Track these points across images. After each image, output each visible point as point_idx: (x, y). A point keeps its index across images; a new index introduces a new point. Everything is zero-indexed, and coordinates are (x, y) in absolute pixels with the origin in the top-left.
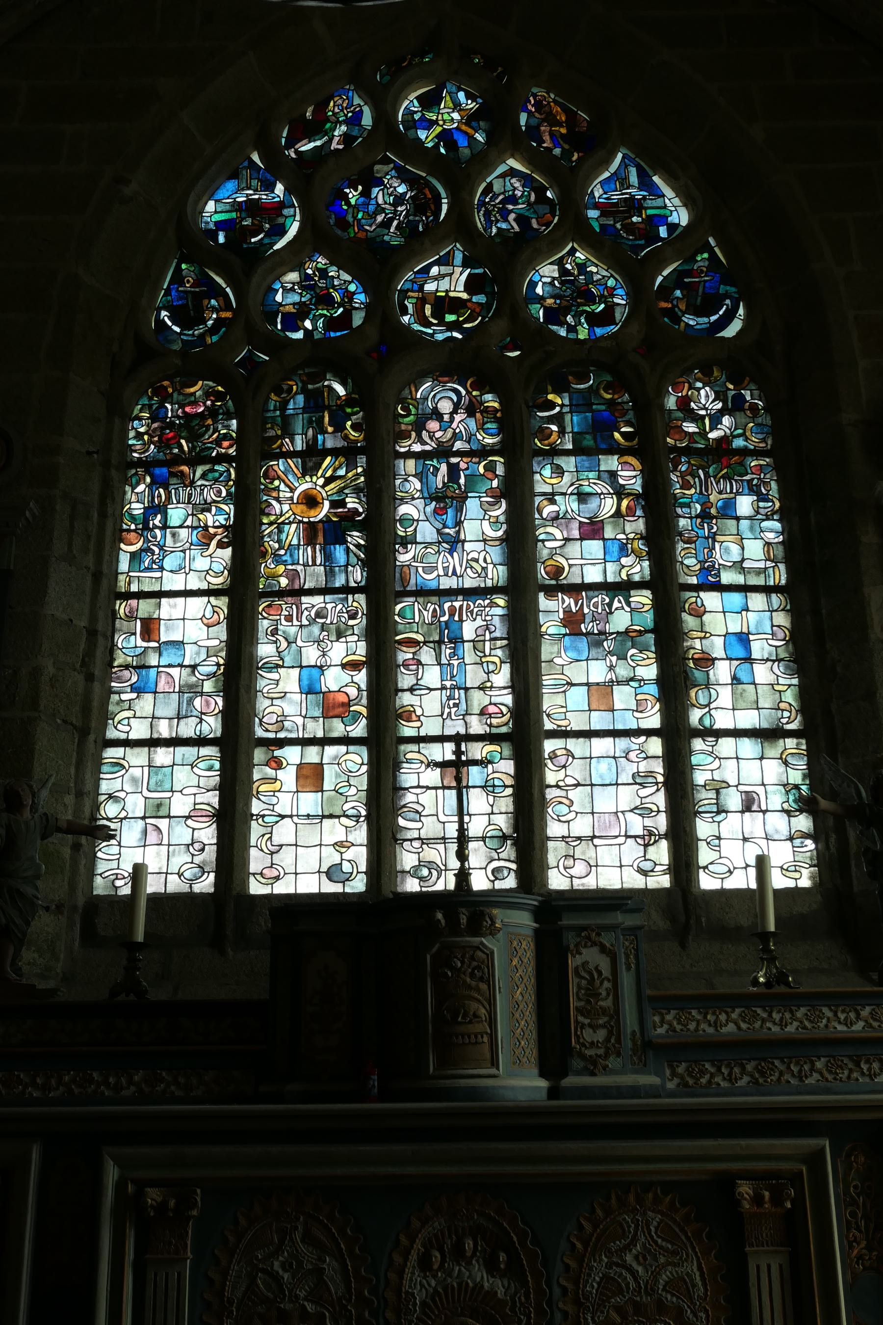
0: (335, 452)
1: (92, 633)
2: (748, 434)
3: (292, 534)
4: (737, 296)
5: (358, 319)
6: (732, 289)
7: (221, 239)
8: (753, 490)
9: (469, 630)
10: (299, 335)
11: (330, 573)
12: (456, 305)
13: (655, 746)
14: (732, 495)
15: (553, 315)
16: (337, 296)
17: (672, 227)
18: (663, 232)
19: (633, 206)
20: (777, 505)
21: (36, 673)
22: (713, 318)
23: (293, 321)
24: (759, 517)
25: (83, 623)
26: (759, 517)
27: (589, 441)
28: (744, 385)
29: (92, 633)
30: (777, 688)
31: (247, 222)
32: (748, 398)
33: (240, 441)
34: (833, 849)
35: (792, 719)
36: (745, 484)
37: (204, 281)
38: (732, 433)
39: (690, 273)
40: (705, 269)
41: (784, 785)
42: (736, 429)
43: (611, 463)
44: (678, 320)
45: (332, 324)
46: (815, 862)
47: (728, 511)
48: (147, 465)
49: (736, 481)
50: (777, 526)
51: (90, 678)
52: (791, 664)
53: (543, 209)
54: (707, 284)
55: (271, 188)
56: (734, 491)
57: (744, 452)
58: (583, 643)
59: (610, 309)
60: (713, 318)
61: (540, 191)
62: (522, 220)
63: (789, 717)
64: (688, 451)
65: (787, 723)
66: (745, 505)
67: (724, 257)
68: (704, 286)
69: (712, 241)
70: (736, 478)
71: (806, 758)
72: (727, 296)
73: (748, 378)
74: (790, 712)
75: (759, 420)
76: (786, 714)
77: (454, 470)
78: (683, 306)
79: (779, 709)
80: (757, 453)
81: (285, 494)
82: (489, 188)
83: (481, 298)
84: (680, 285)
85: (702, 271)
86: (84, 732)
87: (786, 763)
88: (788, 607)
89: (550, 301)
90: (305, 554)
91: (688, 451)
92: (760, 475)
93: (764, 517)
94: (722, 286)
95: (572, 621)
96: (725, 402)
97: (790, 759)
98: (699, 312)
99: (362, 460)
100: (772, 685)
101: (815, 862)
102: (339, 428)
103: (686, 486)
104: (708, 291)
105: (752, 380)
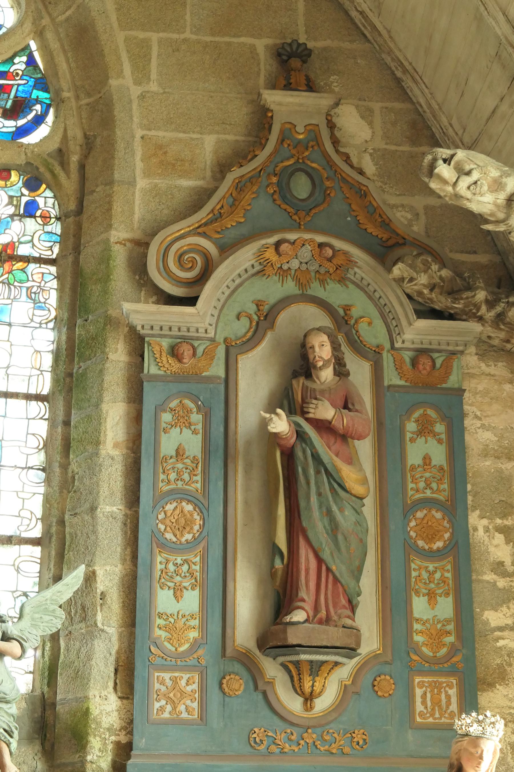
2: (36, 241)
4: (48, 102)
6: (43, 95)
14: (9, 301)
20: (53, 314)
22: (21, 122)
24: (33, 324)
26: (33, 324)
28: (39, 192)
30: (21, 495)
32: (41, 205)
34: (47, 658)
35: (30, 528)
36: (24, 290)
38: (19, 239)
40: (20, 73)
41: (13, 592)
42: (24, 235)
46: (32, 669)
49: (15, 287)
50: (51, 335)
52: (40, 472)
54: (21, 88)
56: (12, 297)
57: (27, 259)
60: (21, 122)
63: (28, 525)
65: (26, 531)
67: (43, 61)
68: (17, 90)
69: (33, 45)
70: (16, 284)
71: (39, 565)
72: (37, 101)
73: (44, 186)
74: (31, 520)
75: (48, 228)
76: (26, 522)
79: (19, 516)
80: (40, 260)
85: (17, 74)
87: (18, 570)
88: (47, 416)
92: (40, 283)
93: (38, 325)
94: (35, 91)
96: (18, 207)
97: (22, 566)
100: (17, 492)
101: (31, 669)
104: (20, 94)
105: (49, 187)
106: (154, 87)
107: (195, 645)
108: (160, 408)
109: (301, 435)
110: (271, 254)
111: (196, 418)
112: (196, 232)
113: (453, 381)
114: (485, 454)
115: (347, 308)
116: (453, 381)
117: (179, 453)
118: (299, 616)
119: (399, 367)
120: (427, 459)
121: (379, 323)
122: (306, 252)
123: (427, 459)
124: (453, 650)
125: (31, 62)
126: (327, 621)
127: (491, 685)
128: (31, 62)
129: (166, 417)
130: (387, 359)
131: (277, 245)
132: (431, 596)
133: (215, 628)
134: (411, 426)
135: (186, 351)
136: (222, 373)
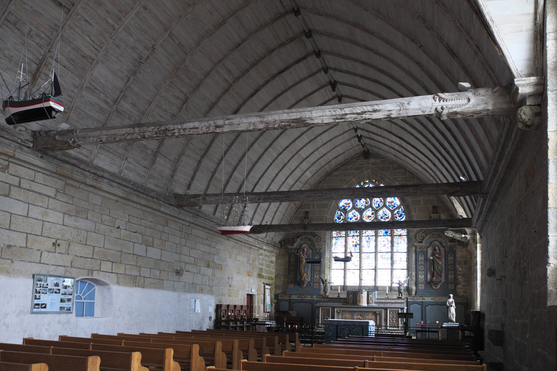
0: (356, 236)
1: (330, 258)
3: (351, 246)
5: (359, 219)
7: (343, 208)
8: (404, 240)
9: (370, 257)
10: (351, 221)
11: (355, 250)
12: (370, 216)
13: (390, 270)
15: (382, 218)
16: (356, 216)
17: (397, 205)
18: (396, 206)
19: (392, 202)
21: (325, 263)
22: (401, 218)
23: (351, 219)
25: (329, 257)
27: (385, 234)
29: (330, 258)
31: (346, 206)
33: (345, 235)
37: (341, 214)
39: (399, 211)
43: (387, 237)
44: (396, 218)
45: (356, 219)
47: (400, 242)
48: (335, 237)
51: (330, 262)
53: (381, 203)
55: (348, 200)
58: (383, 259)
59: (389, 217)
60: (401, 218)
61: (381, 200)
62: (379, 205)
64: (396, 236)
66: (403, 242)
77: (369, 238)
78: (397, 216)
81: (350, 241)
82: (375, 200)
83: (373, 216)
84: (397, 213)
86: (330, 268)
89: (382, 216)
90: (352, 248)
91: (396, 236)
95: (382, 256)
98: (400, 217)
99: (359, 237)
102: (356, 233)
103: (396, 240)
106: (417, 213)
107: (423, 281)
108: (419, 255)
109: (434, 258)
110: (431, 236)
111: (423, 256)
112: (422, 233)
113: (454, 249)
114: (459, 258)
115: (441, 241)
116: (454, 249)
117: (421, 260)
118: (434, 279)
119: (447, 248)
120: (451, 259)
121: (445, 243)
122: (436, 235)
123: (451, 259)
124: (454, 281)
125: (402, 209)
126: (438, 279)
127: (458, 285)
128: (402, 209)
129: (420, 256)
130: (446, 248)
131: (432, 235)
132: (451, 275)
133: (426, 279)
134: (449, 255)
135: (421, 248)
136: (426, 250)
